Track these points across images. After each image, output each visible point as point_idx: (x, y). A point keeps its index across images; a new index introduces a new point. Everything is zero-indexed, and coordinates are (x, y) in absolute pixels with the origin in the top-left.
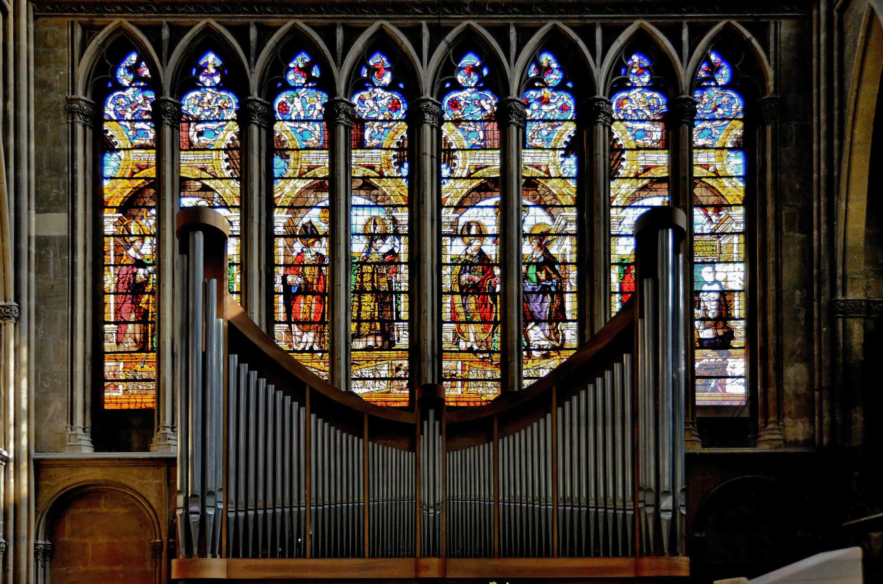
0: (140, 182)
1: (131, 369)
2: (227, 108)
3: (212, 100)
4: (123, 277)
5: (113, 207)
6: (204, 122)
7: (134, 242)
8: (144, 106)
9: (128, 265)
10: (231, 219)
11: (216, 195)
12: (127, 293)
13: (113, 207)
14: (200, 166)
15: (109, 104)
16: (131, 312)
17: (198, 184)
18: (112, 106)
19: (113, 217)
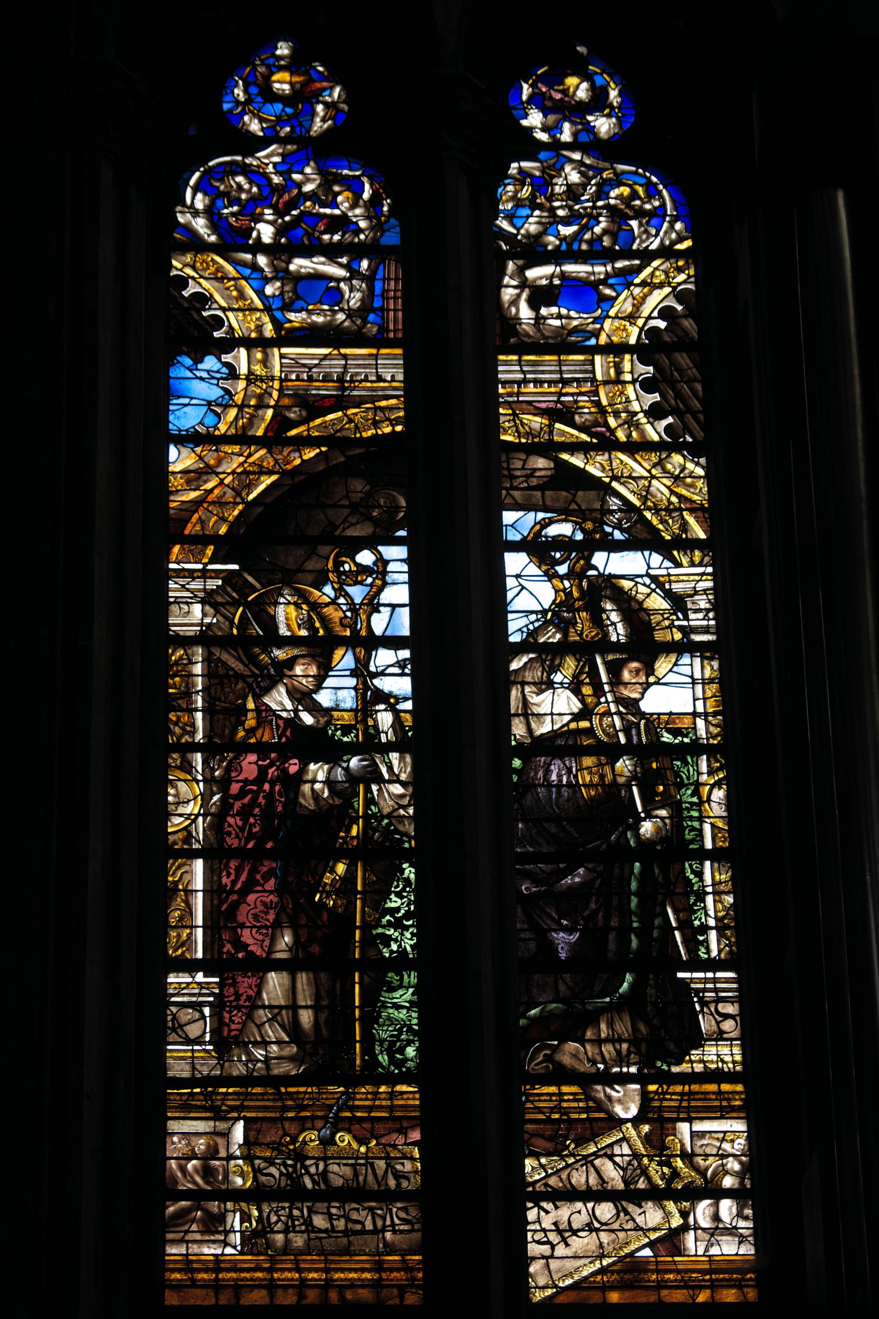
0: (310, 454)
1: (277, 1146)
2: (639, 214)
3: (584, 186)
4: (242, 794)
5: (202, 540)
6: (557, 257)
7: (290, 663)
8: (324, 205)
9: (262, 749)
10: (677, 587)
11: (614, 503)
12: (256, 856)
13: (202, 540)
14: (547, 401)
15: (189, 193)
16: (277, 926)
17: (541, 463)
18: (200, 202)
19: (204, 574)
